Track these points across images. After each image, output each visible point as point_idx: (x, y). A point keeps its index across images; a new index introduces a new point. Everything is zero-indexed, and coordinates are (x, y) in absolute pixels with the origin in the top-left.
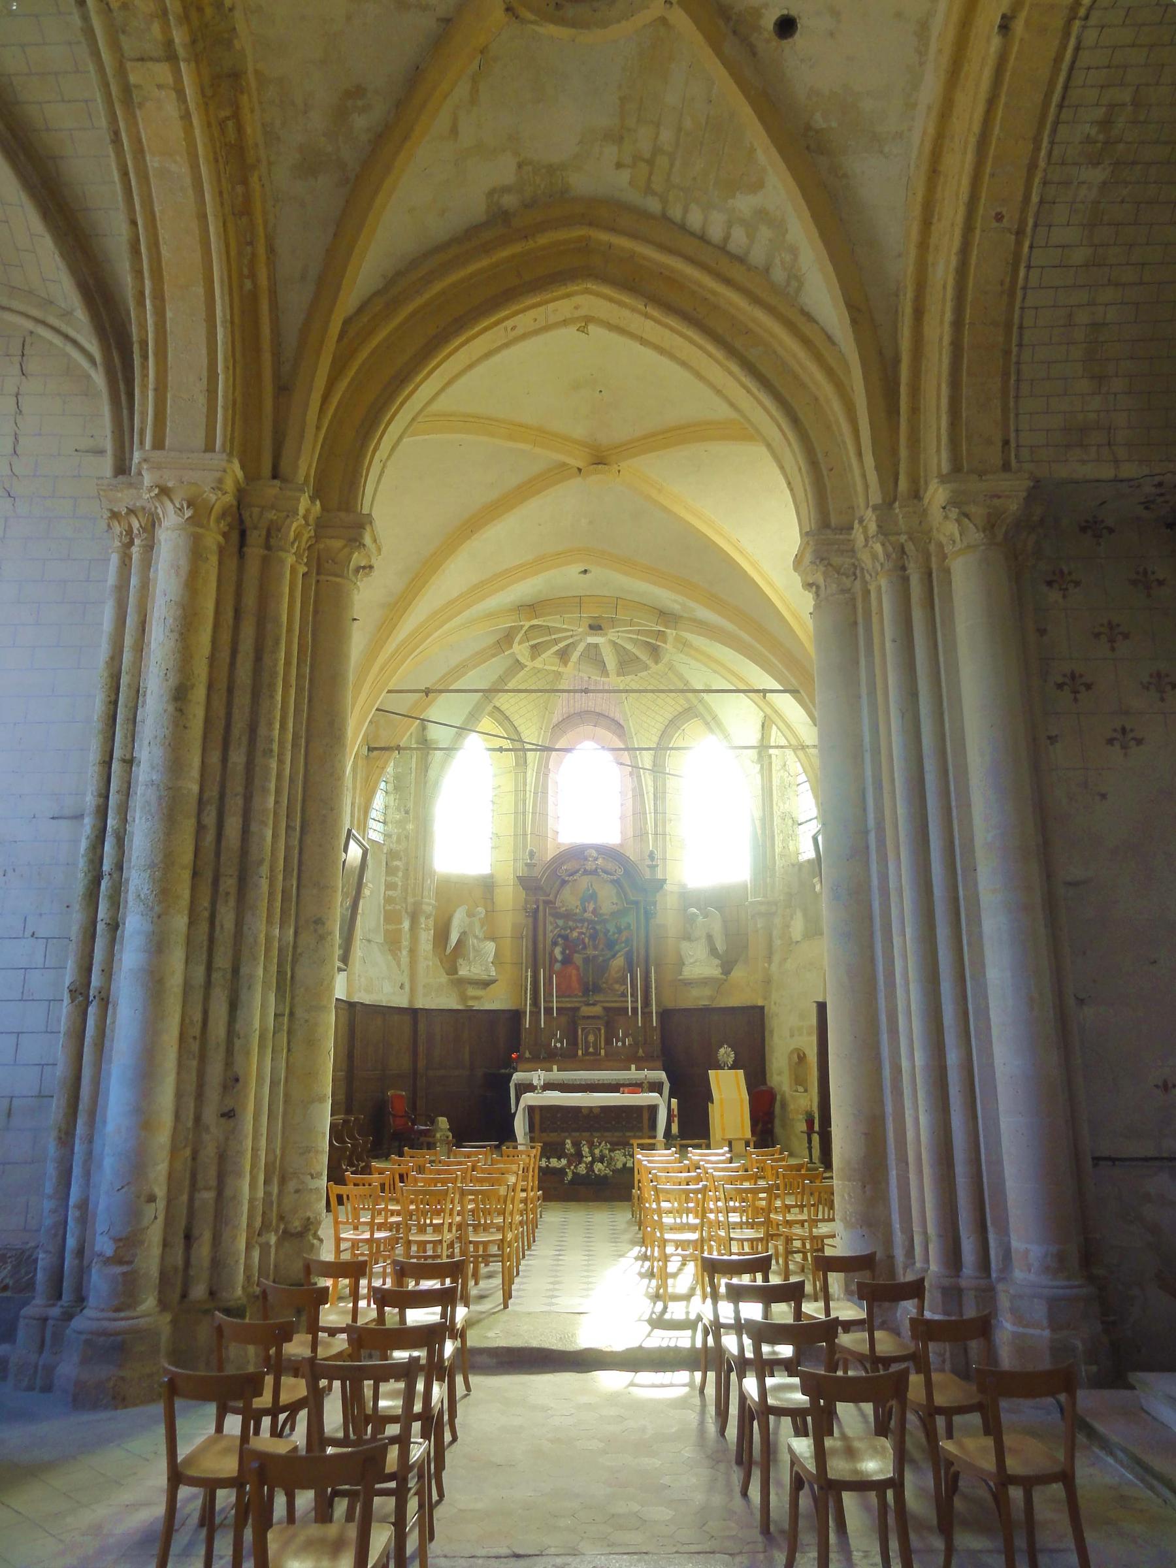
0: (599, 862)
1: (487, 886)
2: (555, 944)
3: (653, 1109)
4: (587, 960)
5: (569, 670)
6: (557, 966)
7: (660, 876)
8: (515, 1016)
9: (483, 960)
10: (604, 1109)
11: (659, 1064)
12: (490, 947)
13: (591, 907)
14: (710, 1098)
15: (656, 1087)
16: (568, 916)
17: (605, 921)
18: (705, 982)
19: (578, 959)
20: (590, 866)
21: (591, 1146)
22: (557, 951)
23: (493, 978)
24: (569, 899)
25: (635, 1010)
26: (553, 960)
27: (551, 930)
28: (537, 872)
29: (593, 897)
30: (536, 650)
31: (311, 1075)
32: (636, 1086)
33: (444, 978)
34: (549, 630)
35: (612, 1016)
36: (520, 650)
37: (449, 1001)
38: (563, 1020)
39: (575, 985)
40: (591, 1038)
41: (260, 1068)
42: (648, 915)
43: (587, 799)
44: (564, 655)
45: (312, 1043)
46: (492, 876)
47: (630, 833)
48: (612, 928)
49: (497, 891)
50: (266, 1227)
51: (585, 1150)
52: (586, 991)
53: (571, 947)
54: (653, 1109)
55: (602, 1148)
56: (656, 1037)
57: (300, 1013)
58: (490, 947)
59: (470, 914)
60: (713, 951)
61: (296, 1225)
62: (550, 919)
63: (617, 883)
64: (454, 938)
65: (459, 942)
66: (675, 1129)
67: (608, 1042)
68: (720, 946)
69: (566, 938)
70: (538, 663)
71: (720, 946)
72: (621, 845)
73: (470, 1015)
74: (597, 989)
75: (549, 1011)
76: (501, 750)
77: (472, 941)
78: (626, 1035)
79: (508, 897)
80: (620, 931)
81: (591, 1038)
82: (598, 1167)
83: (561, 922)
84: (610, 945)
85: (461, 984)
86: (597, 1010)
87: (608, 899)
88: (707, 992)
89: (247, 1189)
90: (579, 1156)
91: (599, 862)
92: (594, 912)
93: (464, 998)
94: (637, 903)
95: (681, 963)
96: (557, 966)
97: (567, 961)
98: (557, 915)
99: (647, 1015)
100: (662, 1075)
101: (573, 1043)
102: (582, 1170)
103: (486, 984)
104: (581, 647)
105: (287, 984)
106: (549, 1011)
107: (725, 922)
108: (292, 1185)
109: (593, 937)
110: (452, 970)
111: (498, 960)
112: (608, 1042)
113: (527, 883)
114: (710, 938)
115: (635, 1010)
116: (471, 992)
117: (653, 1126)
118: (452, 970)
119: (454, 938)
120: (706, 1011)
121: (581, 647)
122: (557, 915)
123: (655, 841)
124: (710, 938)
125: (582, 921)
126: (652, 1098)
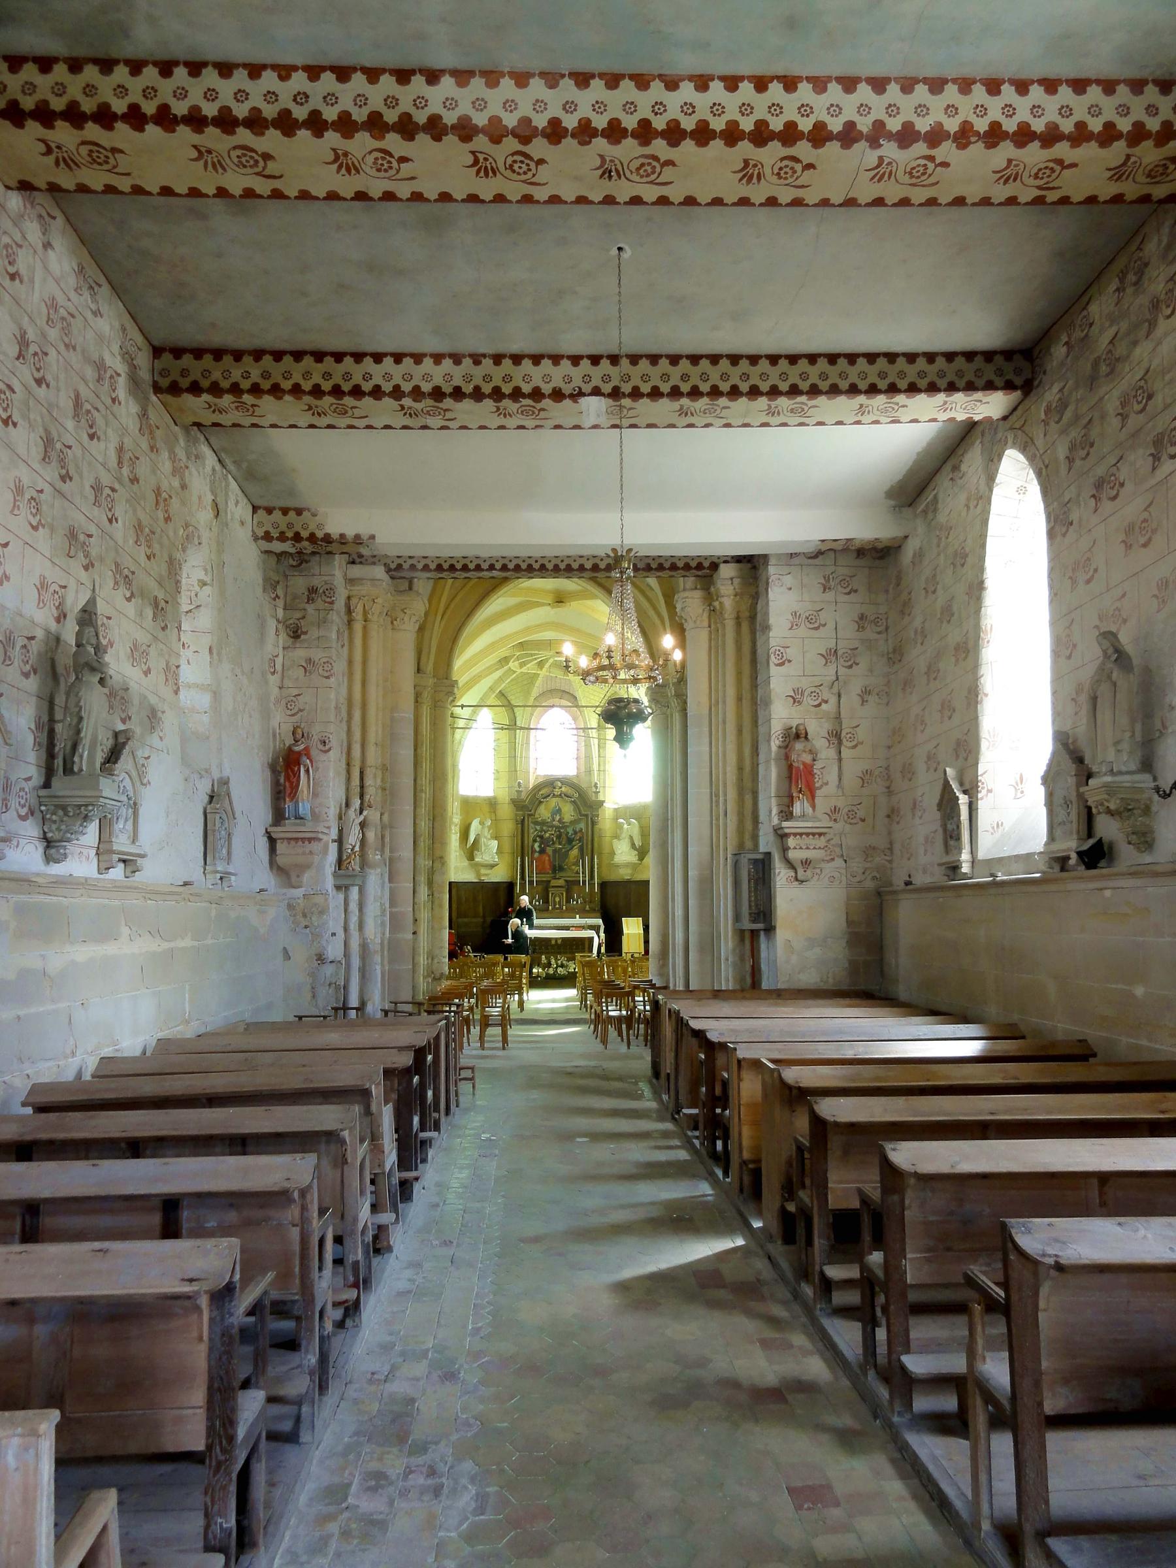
0: (563, 789)
1: (492, 803)
2: (535, 841)
3: (591, 939)
4: (555, 851)
5: (543, 673)
6: (536, 855)
7: (601, 798)
8: (510, 886)
9: (490, 851)
10: (564, 939)
11: (599, 914)
12: (494, 844)
13: (558, 818)
14: (621, 932)
15: (596, 928)
16: (543, 823)
17: (565, 827)
18: (627, 865)
19: (549, 850)
20: (557, 791)
21: (556, 960)
22: (536, 846)
23: (494, 862)
24: (544, 813)
25: (584, 882)
26: (533, 851)
27: (532, 832)
28: (523, 796)
29: (559, 811)
30: (522, 665)
31: (442, 918)
32: (582, 927)
33: (466, 863)
34: (532, 655)
35: (571, 885)
36: (513, 665)
37: (469, 877)
38: (540, 888)
39: (547, 866)
40: (557, 899)
41: (424, 915)
42: (593, 823)
43: (556, 747)
44: (541, 665)
45: (441, 906)
46: (495, 798)
47: (583, 769)
48: (570, 831)
49: (498, 807)
50: (428, 976)
51: (553, 961)
52: (554, 870)
53: (545, 842)
54: (591, 939)
55: (562, 959)
56: (597, 898)
57: (436, 894)
58: (494, 844)
59: (482, 823)
60: (633, 845)
61: (438, 976)
62: (532, 825)
63: (574, 802)
64: (472, 838)
65: (476, 841)
66: (603, 950)
67: (568, 901)
68: (638, 843)
69: (541, 837)
70: (524, 670)
71: (638, 843)
72: (577, 776)
73: (481, 885)
74: (561, 869)
75: (531, 882)
76: (502, 729)
77: (483, 840)
78: (578, 897)
79: (506, 811)
80: (575, 833)
81: (557, 899)
82: (560, 969)
83: (538, 828)
84: (570, 841)
85: (476, 867)
86: (561, 882)
87: (568, 812)
88: (629, 871)
89: (422, 960)
90: (549, 965)
91: (563, 789)
92: (560, 821)
93: (478, 874)
94: (586, 816)
95: (613, 853)
96: (536, 855)
97: (542, 851)
98: (536, 823)
99: (592, 885)
100: (600, 921)
101: (546, 901)
102: (551, 971)
103: (492, 866)
104: (551, 661)
105: (430, 883)
106: (531, 882)
107: (641, 827)
108: (436, 961)
109: (559, 837)
110: (471, 857)
111: (500, 851)
112: (568, 901)
113: (517, 804)
114: (631, 838)
115: (584, 882)
116: (483, 871)
117: (591, 951)
118: (471, 857)
119: (472, 838)
120: (629, 882)
121: (551, 661)
122: (536, 823)
123: (599, 775)
124: (631, 838)
125: (552, 826)
126: (592, 933)
